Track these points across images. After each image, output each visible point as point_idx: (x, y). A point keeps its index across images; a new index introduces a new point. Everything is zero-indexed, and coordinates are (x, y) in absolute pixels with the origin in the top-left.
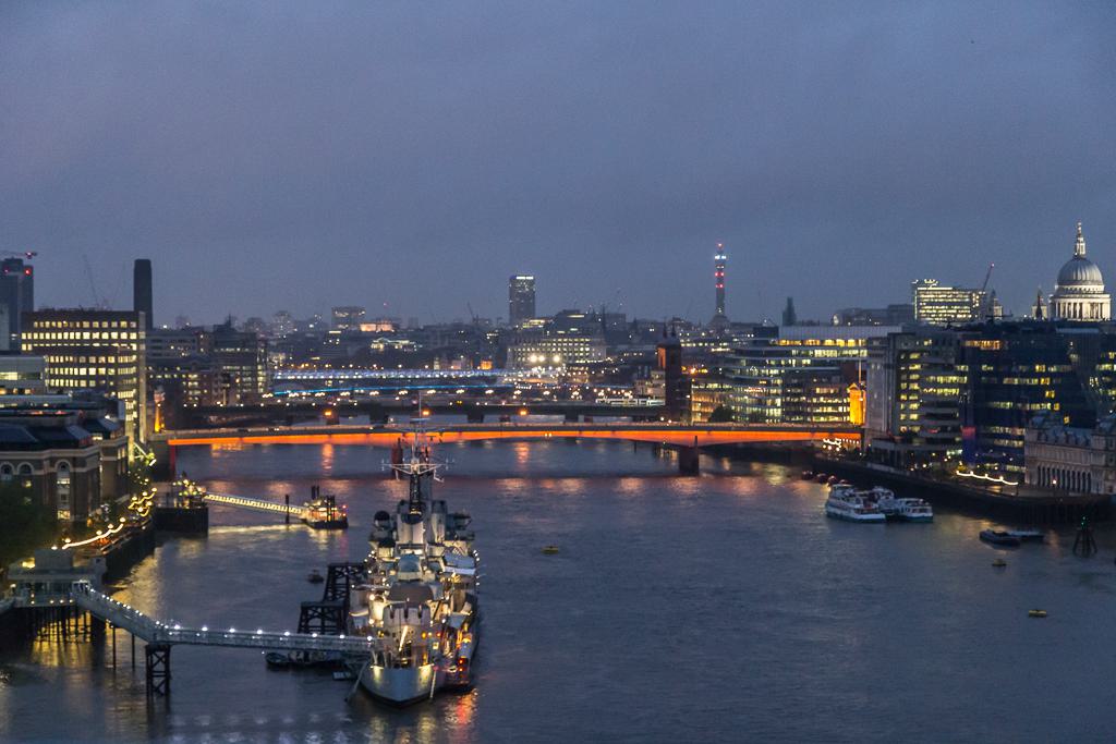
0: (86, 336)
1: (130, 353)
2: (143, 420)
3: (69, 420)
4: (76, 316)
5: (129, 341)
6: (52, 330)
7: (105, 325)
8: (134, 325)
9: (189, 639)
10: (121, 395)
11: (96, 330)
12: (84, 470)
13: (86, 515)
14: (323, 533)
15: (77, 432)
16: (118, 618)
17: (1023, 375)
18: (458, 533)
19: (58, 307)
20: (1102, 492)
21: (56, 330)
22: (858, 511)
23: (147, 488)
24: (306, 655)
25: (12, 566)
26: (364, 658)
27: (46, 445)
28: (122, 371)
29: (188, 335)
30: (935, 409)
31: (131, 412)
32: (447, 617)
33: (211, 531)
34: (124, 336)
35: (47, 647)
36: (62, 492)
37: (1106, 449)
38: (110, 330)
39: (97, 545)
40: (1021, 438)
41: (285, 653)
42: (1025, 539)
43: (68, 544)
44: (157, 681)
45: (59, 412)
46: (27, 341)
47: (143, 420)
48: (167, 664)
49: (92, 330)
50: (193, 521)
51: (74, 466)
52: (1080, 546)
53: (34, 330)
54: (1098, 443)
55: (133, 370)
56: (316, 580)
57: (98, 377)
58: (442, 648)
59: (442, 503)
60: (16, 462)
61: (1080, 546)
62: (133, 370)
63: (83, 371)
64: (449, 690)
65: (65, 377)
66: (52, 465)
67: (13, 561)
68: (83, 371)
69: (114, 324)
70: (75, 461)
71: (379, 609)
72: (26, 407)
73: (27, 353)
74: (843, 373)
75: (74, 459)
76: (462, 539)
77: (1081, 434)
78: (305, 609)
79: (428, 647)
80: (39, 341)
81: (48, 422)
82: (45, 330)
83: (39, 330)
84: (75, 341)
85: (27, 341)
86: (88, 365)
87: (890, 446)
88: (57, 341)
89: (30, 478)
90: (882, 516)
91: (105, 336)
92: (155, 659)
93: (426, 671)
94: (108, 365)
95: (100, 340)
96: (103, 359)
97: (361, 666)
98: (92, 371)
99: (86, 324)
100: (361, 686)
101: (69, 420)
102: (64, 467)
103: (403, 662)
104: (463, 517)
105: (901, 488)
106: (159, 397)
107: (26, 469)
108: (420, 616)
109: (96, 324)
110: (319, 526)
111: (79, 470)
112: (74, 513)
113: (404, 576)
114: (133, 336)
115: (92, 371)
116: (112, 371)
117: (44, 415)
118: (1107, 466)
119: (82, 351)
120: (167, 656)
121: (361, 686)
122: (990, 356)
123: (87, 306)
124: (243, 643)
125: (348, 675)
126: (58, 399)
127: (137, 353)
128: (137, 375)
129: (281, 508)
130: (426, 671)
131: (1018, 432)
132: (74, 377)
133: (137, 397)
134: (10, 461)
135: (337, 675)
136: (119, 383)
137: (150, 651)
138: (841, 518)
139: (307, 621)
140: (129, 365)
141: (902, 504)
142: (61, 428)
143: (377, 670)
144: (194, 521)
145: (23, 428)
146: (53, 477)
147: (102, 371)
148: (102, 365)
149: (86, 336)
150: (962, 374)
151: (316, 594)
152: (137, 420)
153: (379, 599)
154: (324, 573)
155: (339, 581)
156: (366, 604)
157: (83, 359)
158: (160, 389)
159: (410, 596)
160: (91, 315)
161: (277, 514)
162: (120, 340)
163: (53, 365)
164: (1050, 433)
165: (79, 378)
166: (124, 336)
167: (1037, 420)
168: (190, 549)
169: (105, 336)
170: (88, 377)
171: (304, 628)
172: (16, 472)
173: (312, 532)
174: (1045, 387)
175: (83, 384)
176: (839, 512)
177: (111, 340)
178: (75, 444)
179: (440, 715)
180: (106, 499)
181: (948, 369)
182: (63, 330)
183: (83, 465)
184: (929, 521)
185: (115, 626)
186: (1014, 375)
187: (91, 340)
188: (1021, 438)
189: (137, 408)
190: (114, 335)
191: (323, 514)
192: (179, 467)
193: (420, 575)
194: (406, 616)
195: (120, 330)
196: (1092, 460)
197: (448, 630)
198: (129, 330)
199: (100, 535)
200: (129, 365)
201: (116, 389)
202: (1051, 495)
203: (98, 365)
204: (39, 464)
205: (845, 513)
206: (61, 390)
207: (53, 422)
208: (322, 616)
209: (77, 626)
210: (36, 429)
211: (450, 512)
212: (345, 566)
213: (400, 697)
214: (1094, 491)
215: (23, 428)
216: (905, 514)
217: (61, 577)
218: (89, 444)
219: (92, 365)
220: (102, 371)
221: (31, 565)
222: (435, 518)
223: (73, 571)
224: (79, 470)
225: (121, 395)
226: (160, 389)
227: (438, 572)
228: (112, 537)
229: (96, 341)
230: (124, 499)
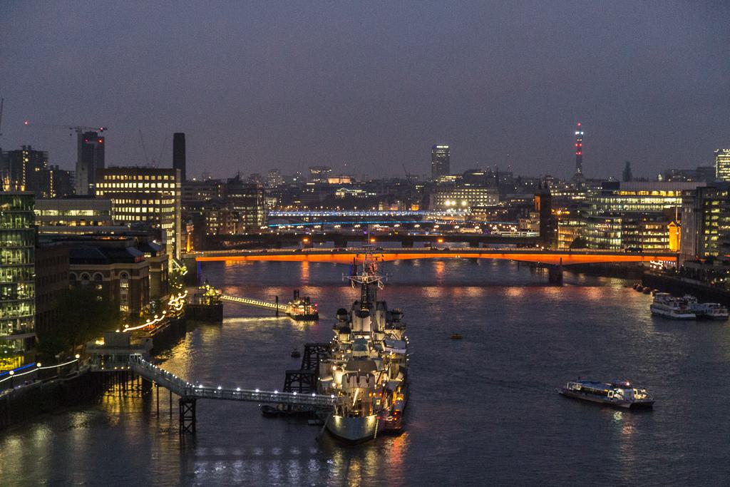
0: (140, 185)
1: (170, 197)
2: (179, 244)
4: (134, 172)
5: (169, 189)
6: (117, 181)
7: (153, 178)
9: (209, 395)
10: (164, 226)
11: (146, 182)
12: (137, 278)
13: (139, 309)
14: (302, 324)
15: (133, 251)
16: (161, 380)
18: (394, 325)
19: (121, 165)
21: (120, 181)
22: (677, 312)
23: (182, 291)
24: (289, 407)
26: (329, 410)
27: (113, 261)
28: (164, 210)
29: (210, 185)
31: (171, 238)
32: (386, 382)
33: (225, 321)
34: (166, 185)
35: (112, 399)
36: (123, 293)
38: (156, 181)
39: (147, 330)
41: (275, 406)
43: (127, 328)
44: (187, 424)
46: (100, 189)
47: (179, 244)
48: (194, 412)
49: (144, 181)
51: (131, 275)
53: (105, 182)
55: (172, 209)
56: (296, 355)
57: (148, 214)
58: (382, 404)
59: (384, 303)
60: (91, 272)
62: (172, 209)
63: (138, 210)
64: (386, 432)
65: (125, 214)
66: (116, 274)
67: (90, 340)
68: (138, 210)
69: (160, 178)
70: (132, 272)
71: (339, 376)
74: (663, 218)
75: (132, 270)
76: (397, 328)
78: (288, 375)
79: (374, 405)
80: (108, 189)
82: (112, 181)
84: (133, 189)
85: (100, 189)
86: (141, 206)
87: (697, 267)
90: (693, 315)
91: (153, 186)
92: (186, 409)
93: (371, 420)
94: (155, 206)
95: (150, 189)
96: (151, 202)
97: (326, 416)
98: (144, 210)
99: (140, 178)
100: (327, 429)
101: (128, 243)
102: (124, 276)
103: (354, 416)
104: (398, 313)
105: (703, 295)
106: (190, 228)
107: (99, 277)
108: (368, 381)
110: (298, 318)
111: (134, 278)
113: (356, 354)
114: (173, 186)
115: (144, 210)
117: (111, 240)
119: (138, 196)
120: (194, 406)
121: (327, 429)
123: (141, 166)
124: (245, 398)
125: (318, 421)
127: (175, 197)
128: (175, 213)
129: (272, 306)
130: (371, 420)
132: (131, 214)
133: (174, 228)
134: (87, 271)
135: (311, 422)
136: (162, 218)
137: (182, 403)
138: (663, 316)
139: (290, 383)
142: (123, 249)
143: (338, 419)
144: (214, 313)
146: (117, 283)
147: (151, 210)
148: (151, 206)
149: (140, 185)
151: (297, 364)
152: (174, 244)
153: (339, 369)
154: (301, 349)
155: (312, 356)
156: (330, 373)
157: (138, 201)
158: (191, 222)
159: (361, 368)
161: (269, 309)
162: (163, 189)
165: (135, 214)
166: (166, 185)
168: (209, 334)
169: (153, 186)
170: (141, 214)
171: (288, 388)
172: (92, 279)
173: (294, 322)
175: (138, 218)
176: (662, 312)
177: (157, 189)
178: (131, 260)
179: (380, 451)
180: (153, 298)
182: (124, 181)
183: (138, 275)
184: (727, 317)
185: (159, 385)
187: (144, 189)
189: (174, 236)
190: (160, 185)
191: (301, 310)
193: (367, 353)
194: (358, 381)
195: (163, 181)
197: (387, 391)
198: (169, 182)
199: (149, 323)
201: (160, 222)
203: (148, 206)
204: (107, 274)
205: (666, 313)
206: (123, 223)
208: (300, 380)
209: (132, 385)
211: (390, 308)
212: (317, 345)
213: (351, 437)
216: (709, 314)
219: (144, 206)
220: (151, 210)
221: (101, 343)
222: (378, 314)
223: (130, 347)
224: (134, 278)
225: (164, 226)
226: (191, 222)
227: (380, 351)
228: (157, 324)
229: (147, 189)
230: (165, 298)
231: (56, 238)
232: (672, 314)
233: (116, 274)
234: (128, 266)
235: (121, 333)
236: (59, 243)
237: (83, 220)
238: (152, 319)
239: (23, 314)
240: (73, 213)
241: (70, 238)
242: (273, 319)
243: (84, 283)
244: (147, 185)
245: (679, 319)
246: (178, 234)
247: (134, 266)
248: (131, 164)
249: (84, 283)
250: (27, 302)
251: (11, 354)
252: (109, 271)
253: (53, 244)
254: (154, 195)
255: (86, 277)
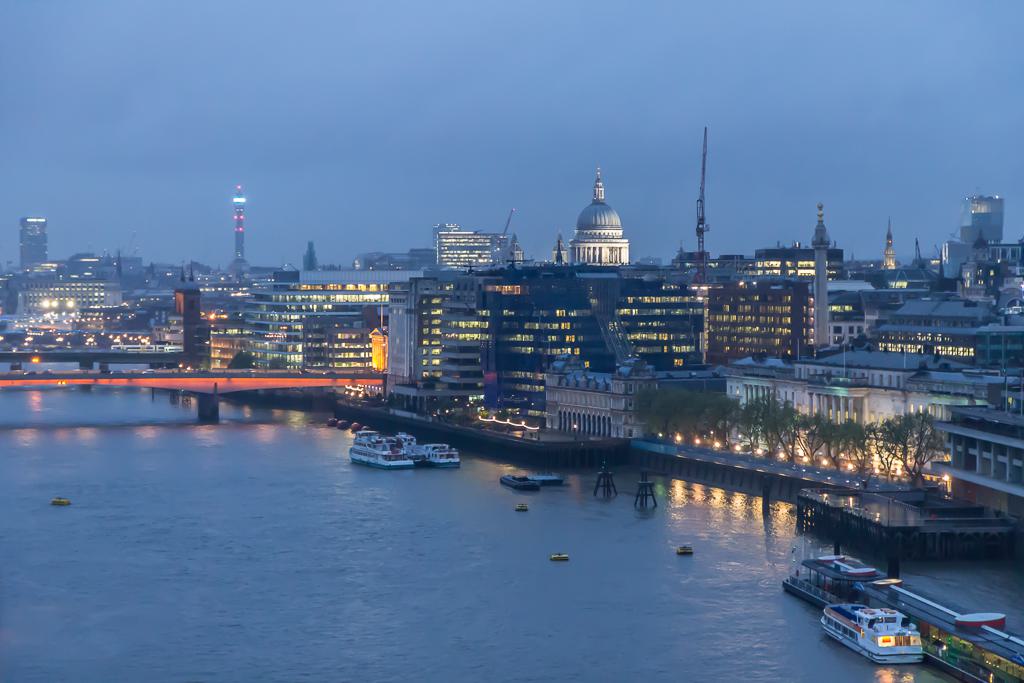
17: (545, 320)
20: (622, 436)
22: (386, 457)
30: (458, 355)
37: (626, 394)
40: (542, 383)
42: (544, 483)
52: (600, 490)
54: (618, 387)
61: (600, 490)
77: (601, 379)
87: (412, 392)
90: (410, 462)
105: (424, 434)
118: (625, 410)
122: (512, 301)
131: (540, 376)
138: (368, 465)
141: (427, 450)
150: (483, 319)
164: (570, 378)
167: (558, 364)
174: (566, 332)
176: (365, 459)
181: (470, 314)
184: (458, 463)
186: (536, 320)
188: (542, 383)
196: (612, 404)
202: (572, 439)
205: (372, 460)
214: (614, 435)
216: (433, 459)
232: (382, 462)
245: (390, 468)
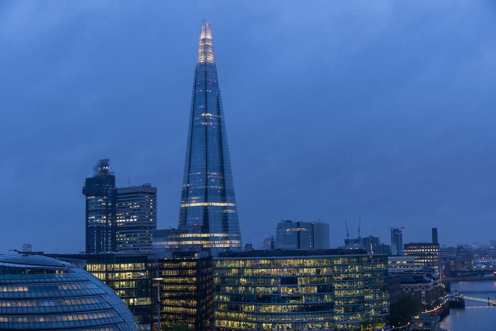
0: (423, 250)
1: (436, 255)
3: (424, 275)
5: (436, 252)
6: (413, 249)
7: (429, 247)
8: (437, 247)
10: (435, 268)
11: (426, 249)
13: (430, 302)
15: (427, 279)
19: (414, 242)
21: (414, 249)
23: (445, 295)
25: (412, 317)
27: (417, 282)
29: (450, 250)
31: (438, 272)
36: (423, 296)
38: (430, 249)
39: (434, 312)
43: (426, 311)
45: (421, 273)
46: (406, 252)
49: (425, 249)
50: (459, 305)
51: (426, 288)
53: (407, 249)
57: (427, 262)
63: (423, 261)
66: (420, 288)
67: (413, 316)
68: (423, 261)
69: (431, 247)
72: (410, 271)
73: (406, 256)
75: (426, 286)
81: (417, 275)
82: (411, 249)
83: (409, 249)
84: (420, 252)
85: (406, 252)
86: (424, 259)
88: (411, 252)
89: (414, 292)
91: (429, 250)
94: (430, 259)
95: (427, 251)
99: (423, 247)
101: (424, 275)
102: (423, 289)
106: (444, 268)
107: (412, 289)
109: (426, 247)
111: (428, 289)
112: (427, 302)
114: (437, 250)
115: (426, 261)
116: (431, 261)
119: (422, 255)
123: (423, 242)
126: (420, 268)
129: (487, 301)
132: (420, 262)
133: (439, 268)
136: (434, 264)
140: (436, 259)
142: (422, 277)
144: (459, 305)
145: (411, 277)
146: (420, 292)
148: (428, 259)
149: (423, 250)
152: (439, 275)
157: (423, 257)
158: (444, 266)
160: (425, 244)
162: (433, 251)
163: (416, 259)
165: (422, 262)
166: (434, 250)
168: (458, 314)
169: (429, 250)
170: (424, 262)
178: (426, 282)
180: (435, 298)
182: (416, 249)
183: (429, 288)
187: (425, 252)
189: (439, 271)
190: (431, 250)
192: (452, 289)
195: (433, 249)
198: (435, 249)
199: (435, 309)
200: (436, 259)
203: (427, 259)
206: (419, 266)
207: (420, 275)
210: (415, 278)
215: (411, 277)
217: (427, 321)
218: (430, 281)
221: (418, 317)
223: (430, 319)
224: (428, 289)
225: (435, 268)
226: (444, 266)
228: (438, 309)
229: (426, 252)
230: (440, 298)
231: (394, 273)
233: (420, 288)
234: (424, 285)
235: (424, 314)
236: (396, 275)
237: (402, 265)
238: (436, 307)
239: (385, 305)
240: (398, 262)
241: (399, 273)
242: (487, 307)
243: (407, 292)
244: (426, 250)
246: (440, 270)
247: (427, 284)
248: (418, 242)
249: (407, 292)
250: (386, 301)
251: (380, 322)
252: (416, 287)
253: (393, 276)
254: (429, 254)
255: (407, 289)
